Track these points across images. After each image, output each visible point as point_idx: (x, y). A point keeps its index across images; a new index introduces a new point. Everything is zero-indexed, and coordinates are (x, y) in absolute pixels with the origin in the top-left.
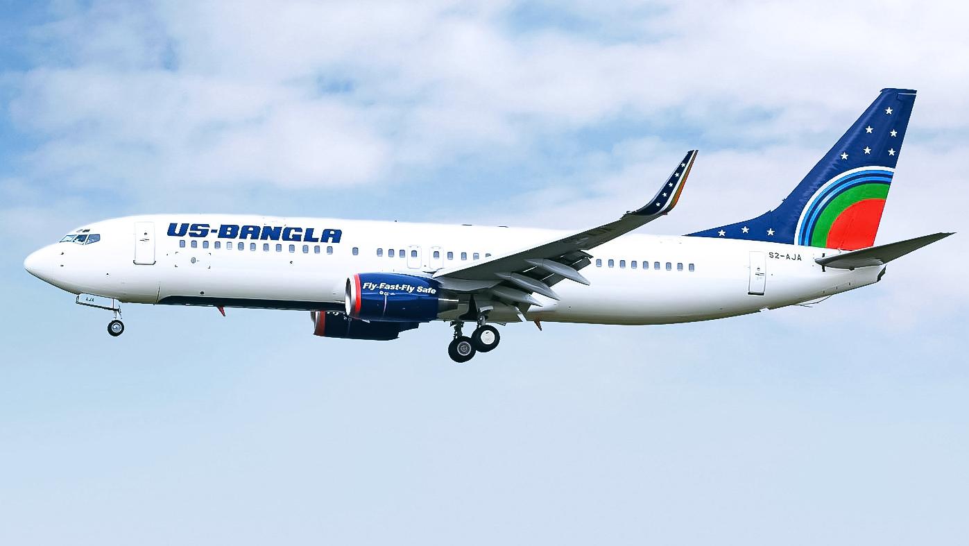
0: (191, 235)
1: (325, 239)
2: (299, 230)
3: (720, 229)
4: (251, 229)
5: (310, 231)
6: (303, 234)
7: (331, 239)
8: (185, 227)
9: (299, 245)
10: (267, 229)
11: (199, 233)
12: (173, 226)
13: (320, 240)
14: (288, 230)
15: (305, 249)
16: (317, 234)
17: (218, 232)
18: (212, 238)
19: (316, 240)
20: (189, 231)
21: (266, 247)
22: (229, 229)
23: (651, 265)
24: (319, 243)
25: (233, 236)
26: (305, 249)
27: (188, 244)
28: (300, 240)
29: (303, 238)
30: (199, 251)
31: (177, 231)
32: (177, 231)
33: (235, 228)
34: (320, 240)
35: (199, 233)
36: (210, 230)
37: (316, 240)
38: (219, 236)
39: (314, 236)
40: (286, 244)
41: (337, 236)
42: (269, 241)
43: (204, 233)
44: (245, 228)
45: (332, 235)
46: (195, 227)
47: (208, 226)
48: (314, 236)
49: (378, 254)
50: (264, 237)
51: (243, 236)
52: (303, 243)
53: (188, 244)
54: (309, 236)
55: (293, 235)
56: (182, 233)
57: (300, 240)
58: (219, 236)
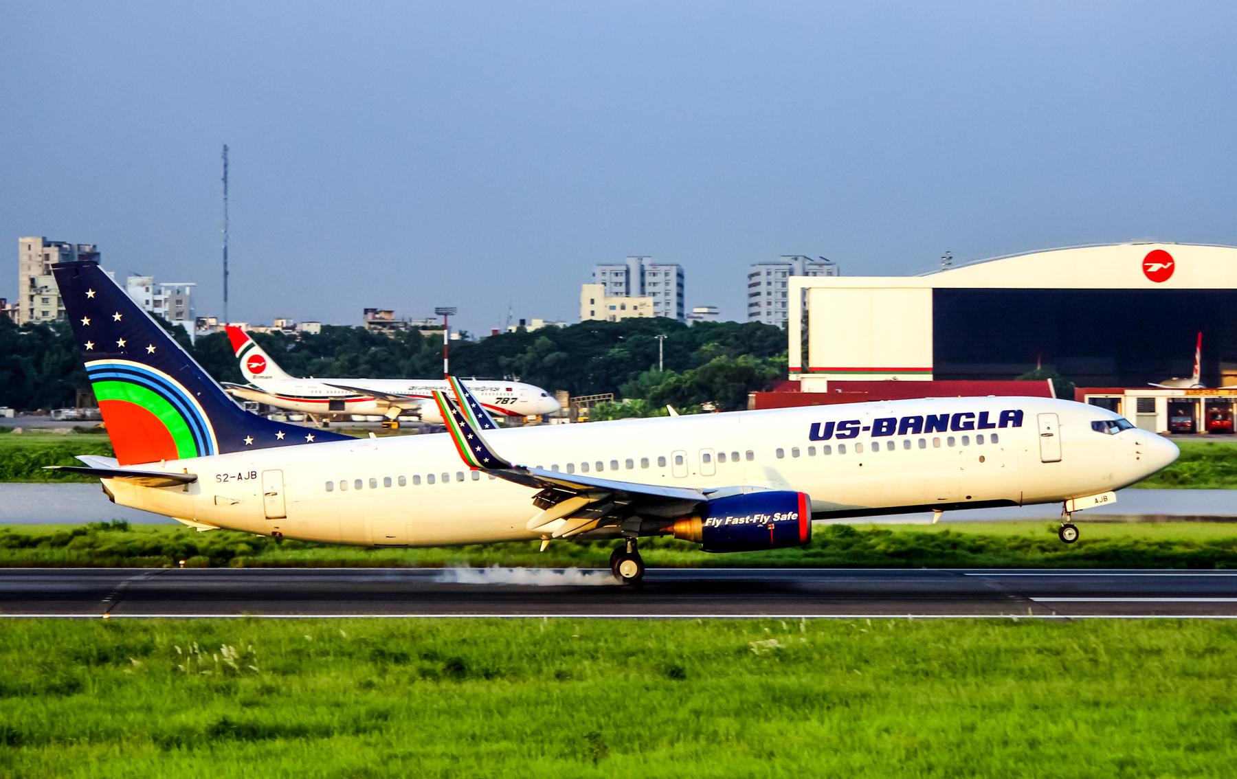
0: (839, 436)
1: (1003, 424)
2: (971, 415)
3: (473, 433)
4: (912, 421)
5: (984, 416)
6: (976, 420)
7: (910, 430)
8: (830, 426)
9: (972, 434)
10: (932, 419)
11: (848, 433)
12: (815, 427)
13: (997, 425)
14: (957, 417)
15: (980, 439)
16: (994, 418)
17: (871, 429)
18: (865, 437)
19: (993, 426)
20: (835, 432)
21: (907, 444)
22: (885, 424)
23: (743, 456)
24: (997, 430)
25: (890, 431)
26: (980, 439)
27: (835, 449)
28: (973, 429)
29: (976, 425)
30: (988, 448)
31: (821, 434)
32: (821, 434)
33: (892, 421)
34: (997, 425)
35: (848, 433)
36: (861, 426)
37: (993, 426)
38: (874, 435)
39: (990, 421)
40: (958, 435)
41: (1018, 418)
42: (935, 433)
43: (855, 433)
44: (905, 421)
45: (911, 425)
46: (842, 426)
47: (858, 422)
48: (990, 421)
49: (705, 461)
50: (928, 430)
51: (903, 431)
52: (976, 432)
53: (835, 449)
54: (984, 422)
56: (828, 435)
57: (973, 429)
58: (874, 435)
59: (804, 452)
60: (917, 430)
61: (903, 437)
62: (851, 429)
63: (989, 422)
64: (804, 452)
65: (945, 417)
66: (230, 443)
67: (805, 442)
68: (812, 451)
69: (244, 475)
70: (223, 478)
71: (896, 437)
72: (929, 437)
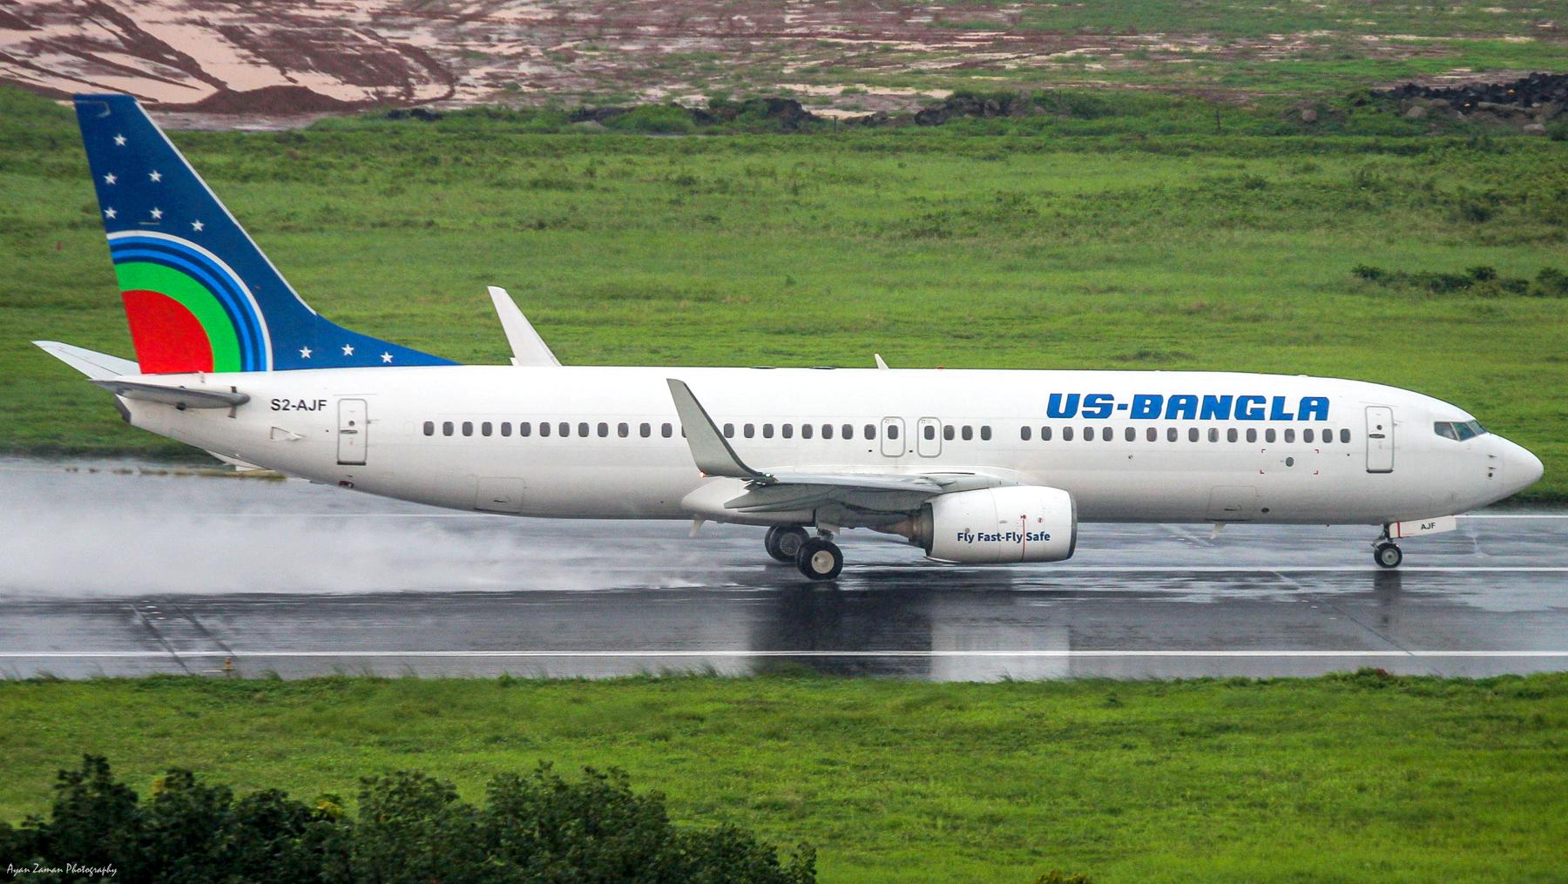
0: (1087, 415)
1: (1303, 416)
2: (1260, 399)
4: (1183, 401)
5: (1279, 402)
6: (1268, 408)
9: (1260, 427)
10: (1209, 400)
11: (1097, 410)
12: (1055, 399)
14: (1243, 401)
16: (1292, 407)
19: (1289, 417)
20: (1081, 408)
25: (1155, 413)
29: (1267, 414)
31: (1062, 410)
32: (1062, 410)
33: (1157, 400)
34: (1296, 417)
35: (1097, 410)
36: (1115, 403)
37: (1289, 417)
40: (1242, 426)
42: (1213, 422)
43: (1106, 412)
44: (1175, 399)
46: (1090, 400)
50: (1205, 416)
51: (1171, 415)
54: (1278, 413)
55: (1252, 410)
56: (1070, 412)
59: (1036, 434)
60: (1190, 415)
61: (1171, 423)
62: (1101, 406)
63: (1285, 411)
64: (1036, 434)
65: (1227, 399)
66: (287, 360)
67: (1038, 418)
68: (1047, 434)
69: (309, 404)
70: (282, 405)
71: (1161, 424)
72: (1204, 426)
